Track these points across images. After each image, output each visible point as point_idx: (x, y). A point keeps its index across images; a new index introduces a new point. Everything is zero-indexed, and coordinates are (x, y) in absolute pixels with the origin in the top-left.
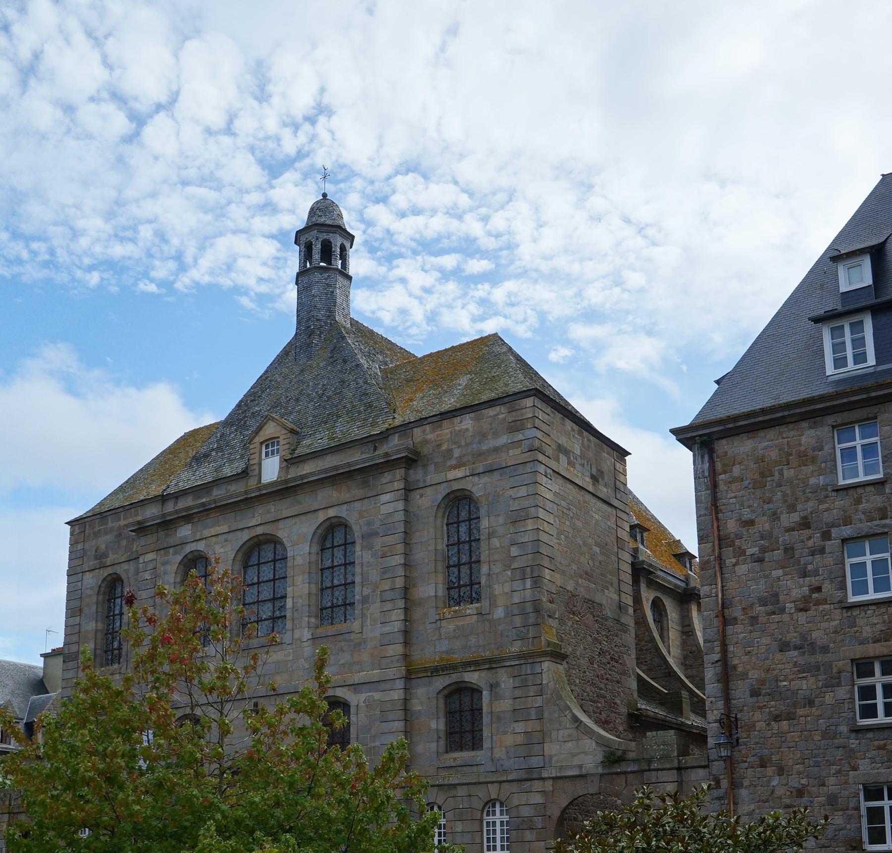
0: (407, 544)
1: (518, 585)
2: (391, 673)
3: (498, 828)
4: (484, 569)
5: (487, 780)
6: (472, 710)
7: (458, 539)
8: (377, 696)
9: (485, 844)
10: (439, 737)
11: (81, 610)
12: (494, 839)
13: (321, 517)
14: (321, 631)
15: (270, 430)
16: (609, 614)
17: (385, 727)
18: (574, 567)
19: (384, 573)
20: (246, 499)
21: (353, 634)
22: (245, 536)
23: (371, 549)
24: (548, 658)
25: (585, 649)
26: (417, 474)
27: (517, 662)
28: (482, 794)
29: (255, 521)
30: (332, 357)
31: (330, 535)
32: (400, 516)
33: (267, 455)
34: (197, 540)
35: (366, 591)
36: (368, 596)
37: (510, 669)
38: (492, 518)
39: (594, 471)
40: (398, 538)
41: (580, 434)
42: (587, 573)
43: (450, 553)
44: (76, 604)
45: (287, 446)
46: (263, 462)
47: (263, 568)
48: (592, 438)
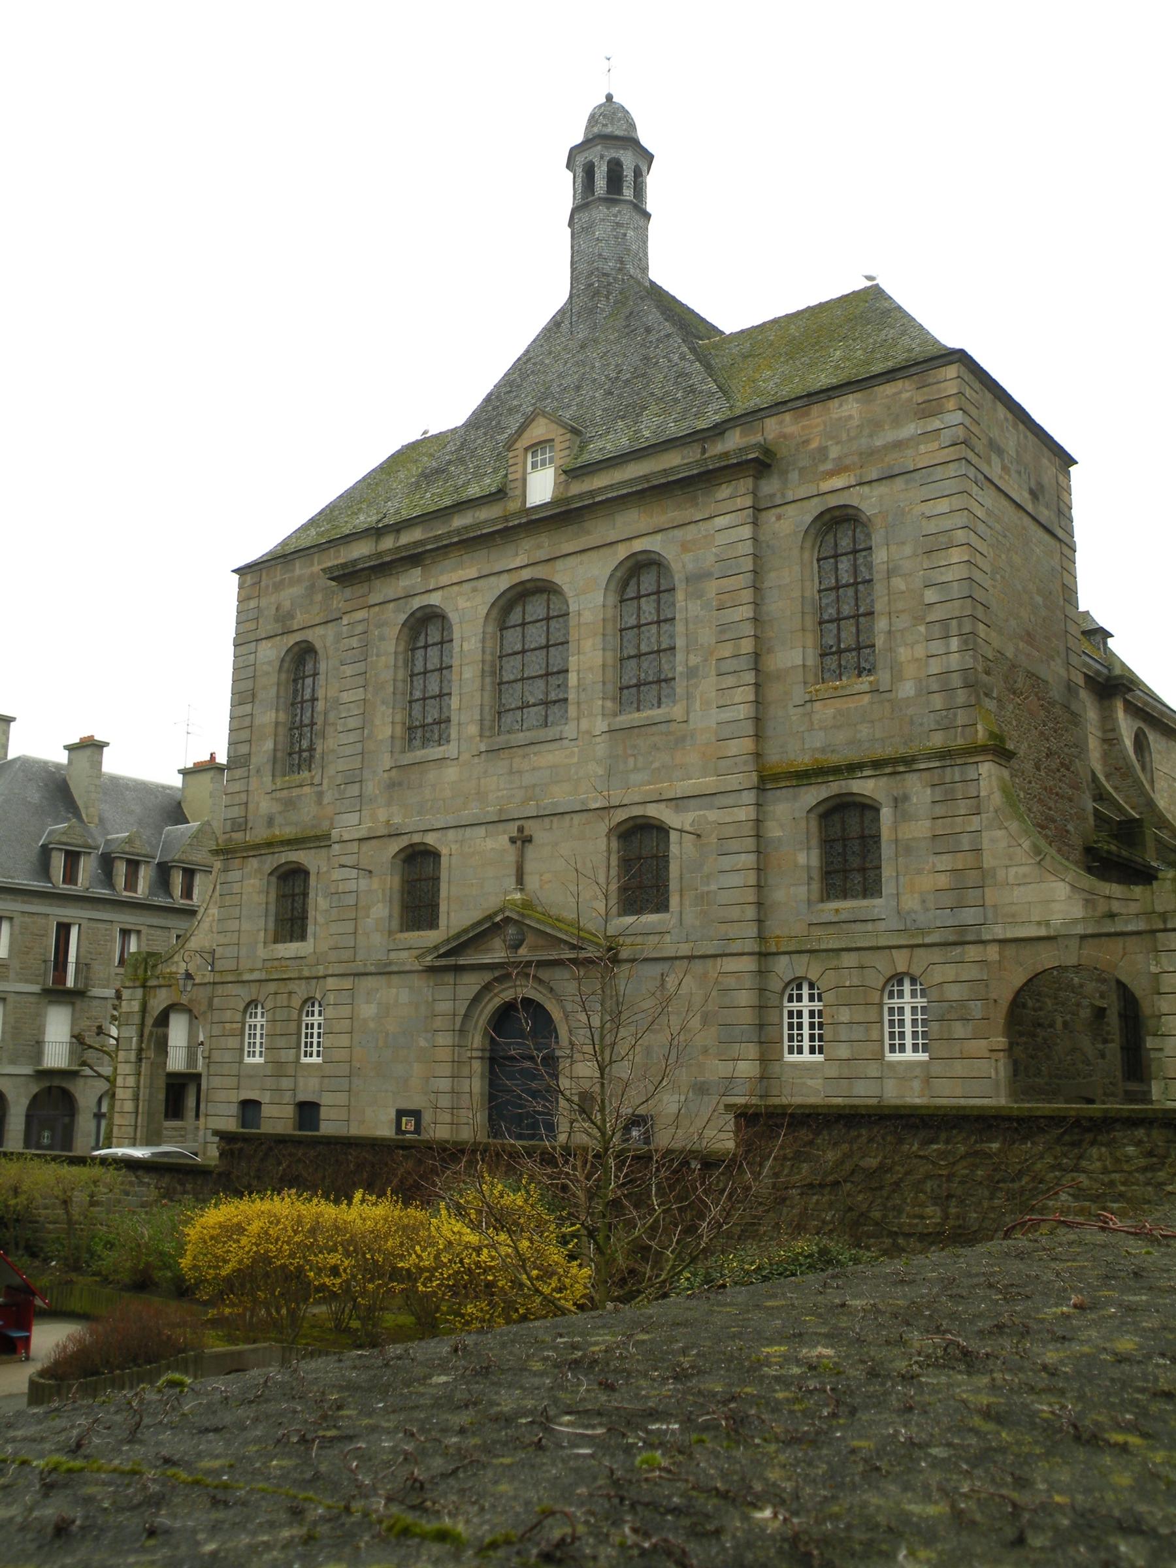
0: (756, 588)
1: (936, 647)
2: (733, 782)
3: (908, 1017)
4: (881, 624)
5: (890, 944)
6: (862, 837)
7: (837, 580)
8: (712, 815)
9: (887, 1042)
10: (810, 878)
11: (253, 695)
12: (902, 1035)
13: (622, 552)
14: (624, 720)
15: (540, 430)
16: (1057, 698)
17: (726, 862)
18: (1013, 623)
19: (722, 632)
20: (507, 529)
21: (674, 724)
22: (504, 583)
23: (700, 597)
24: (990, 757)
25: (1030, 747)
26: (770, 486)
27: (937, 764)
28: (882, 965)
29: (517, 561)
30: (628, 326)
31: (634, 580)
32: (748, 547)
33: (534, 466)
34: (430, 591)
35: (694, 660)
36: (697, 667)
37: (925, 775)
38: (893, 548)
39: (1033, 484)
40: (745, 580)
41: (1015, 426)
42: (1029, 634)
43: (824, 601)
44: (249, 684)
45: (567, 452)
46: (529, 478)
47: (531, 630)
48: (1029, 434)
